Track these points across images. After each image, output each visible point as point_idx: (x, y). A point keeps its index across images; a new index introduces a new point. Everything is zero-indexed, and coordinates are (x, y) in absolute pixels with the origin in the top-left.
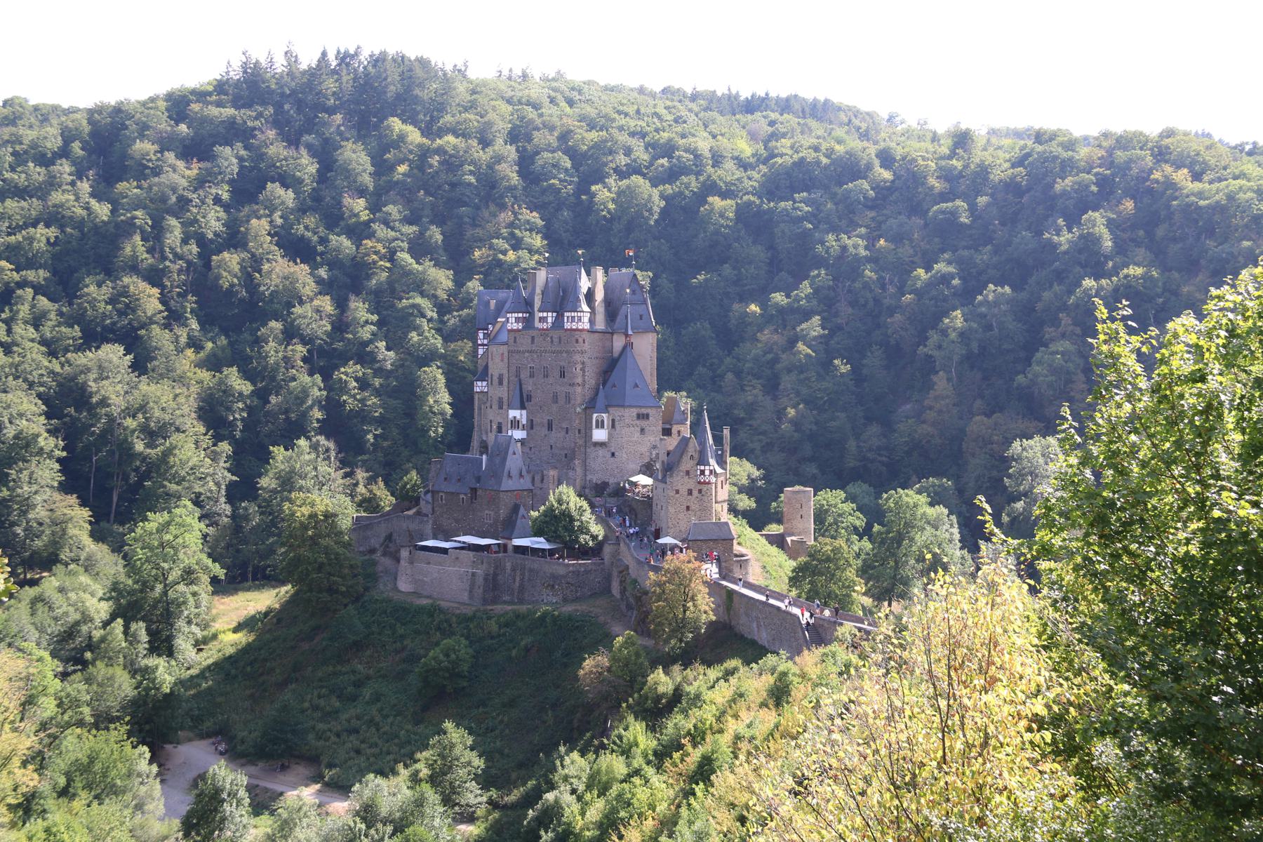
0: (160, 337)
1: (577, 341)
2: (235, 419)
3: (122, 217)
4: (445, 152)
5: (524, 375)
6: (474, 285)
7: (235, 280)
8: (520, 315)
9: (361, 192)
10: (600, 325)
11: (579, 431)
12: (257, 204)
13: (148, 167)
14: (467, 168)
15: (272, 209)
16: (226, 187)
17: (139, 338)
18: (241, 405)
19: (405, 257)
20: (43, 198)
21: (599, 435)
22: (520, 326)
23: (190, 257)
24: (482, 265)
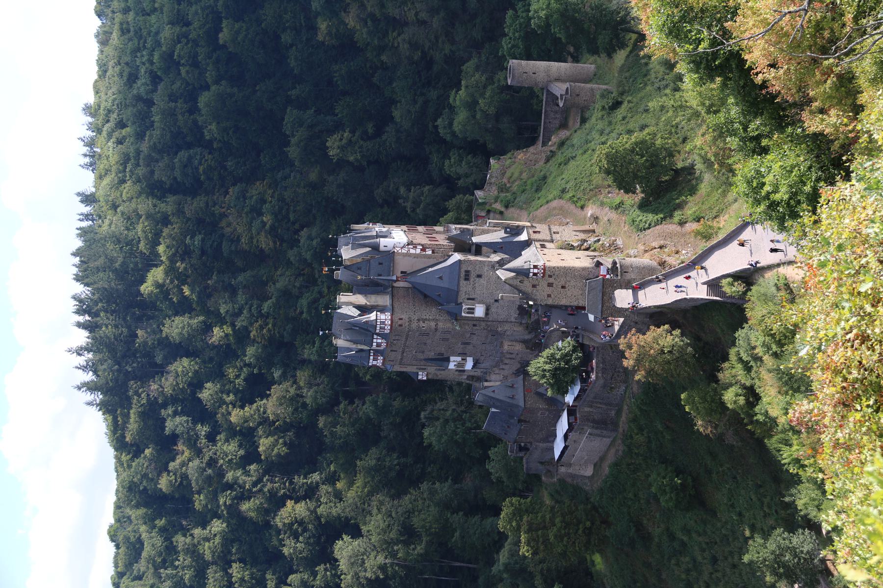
0: (328, 509)
1: (401, 325)
2: (398, 464)
3: (225, 512)
4: (174, 255)
5: (421, 356)
6: (292, 255)
7: (281, 441)
8: (372, 358)
9: (207, 328)
10: (384, 300)
11: (474, 325)
12: (216, 414)
13: (181, 482)
14: (188, 241)
15: (222, 402)
16: (199, 427)
17: (327, 522)
18: (388, 459)
19: (266, 306)
20: (207, 564)
21: (480, 311)
22: (380, 358)
23: (261, 471)
24: (275, 242)
